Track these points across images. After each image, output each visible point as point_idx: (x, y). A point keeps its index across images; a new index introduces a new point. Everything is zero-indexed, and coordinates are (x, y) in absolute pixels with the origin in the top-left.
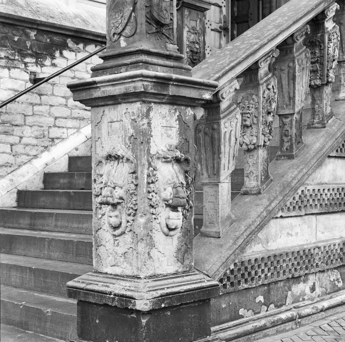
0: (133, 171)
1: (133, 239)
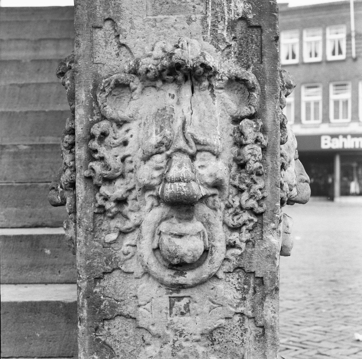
0: (253, 112)
1: (244, 291)
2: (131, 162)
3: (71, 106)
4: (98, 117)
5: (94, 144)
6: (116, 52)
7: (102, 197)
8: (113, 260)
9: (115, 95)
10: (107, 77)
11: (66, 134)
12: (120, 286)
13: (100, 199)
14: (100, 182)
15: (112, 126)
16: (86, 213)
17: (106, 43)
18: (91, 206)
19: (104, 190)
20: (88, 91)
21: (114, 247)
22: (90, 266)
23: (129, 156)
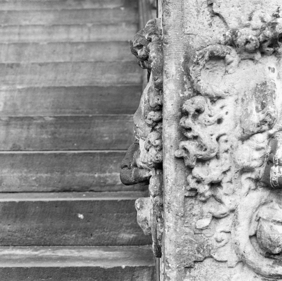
2: (226, 141)
3: (155, 80)
4: (190, 93)
5: (188, 122)
6: (209, 22)
7: (195, 180)
8: (205, 248)
9: (208, 69)
10: (200, 49)
11: (150, 111)
12: (212, 276)
13: (193, 182)
14: (194, 163)
15: (207, 103)
16: (175, 197)
17: (198, 12)
18: (181, 189)
19: (198, 171)
20: (179, 64)
21: (206, 234)
22: (180, 254)
23: (224, 134)
